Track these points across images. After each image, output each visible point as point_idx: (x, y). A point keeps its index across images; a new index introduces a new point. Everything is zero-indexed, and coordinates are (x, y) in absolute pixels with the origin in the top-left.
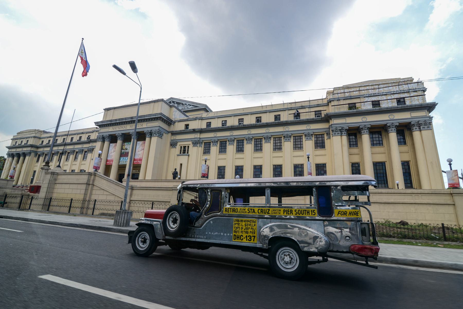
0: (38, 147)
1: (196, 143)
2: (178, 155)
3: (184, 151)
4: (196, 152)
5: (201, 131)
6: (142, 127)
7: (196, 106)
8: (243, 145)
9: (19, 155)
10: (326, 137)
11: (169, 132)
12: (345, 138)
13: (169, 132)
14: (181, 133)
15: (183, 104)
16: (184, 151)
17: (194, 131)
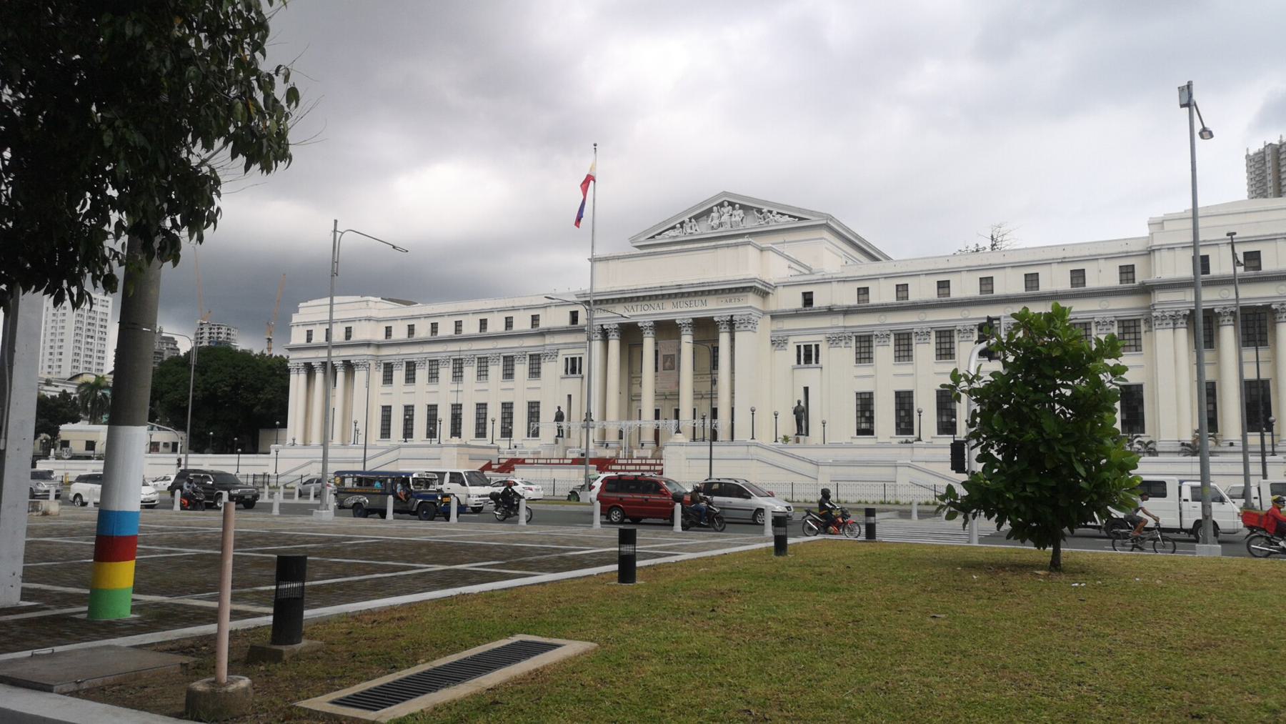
0: (379, 346)
1: (834, 340)
2: (794, 368)
3: (808, 355)
4: (838, 359)
5: (847, 312)
6: (704, 308)
7: (801, 219)
8: (951, 342)
9: (329, 369)
10: (1143, 328)
11: (764, 313)
12: (1182, 333)
13: (764, 313)
14: (795, 314)
15: (760, 211)
16: (808, 355)
17: (830, 311)
